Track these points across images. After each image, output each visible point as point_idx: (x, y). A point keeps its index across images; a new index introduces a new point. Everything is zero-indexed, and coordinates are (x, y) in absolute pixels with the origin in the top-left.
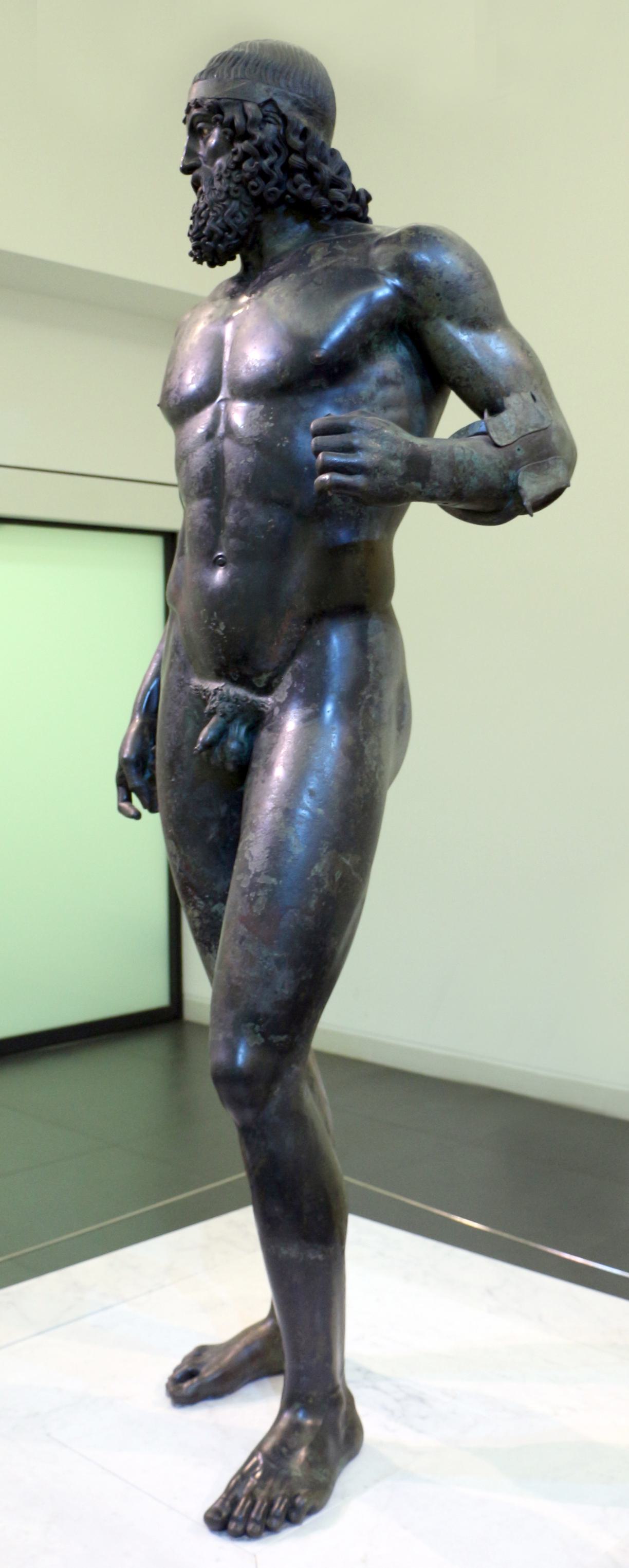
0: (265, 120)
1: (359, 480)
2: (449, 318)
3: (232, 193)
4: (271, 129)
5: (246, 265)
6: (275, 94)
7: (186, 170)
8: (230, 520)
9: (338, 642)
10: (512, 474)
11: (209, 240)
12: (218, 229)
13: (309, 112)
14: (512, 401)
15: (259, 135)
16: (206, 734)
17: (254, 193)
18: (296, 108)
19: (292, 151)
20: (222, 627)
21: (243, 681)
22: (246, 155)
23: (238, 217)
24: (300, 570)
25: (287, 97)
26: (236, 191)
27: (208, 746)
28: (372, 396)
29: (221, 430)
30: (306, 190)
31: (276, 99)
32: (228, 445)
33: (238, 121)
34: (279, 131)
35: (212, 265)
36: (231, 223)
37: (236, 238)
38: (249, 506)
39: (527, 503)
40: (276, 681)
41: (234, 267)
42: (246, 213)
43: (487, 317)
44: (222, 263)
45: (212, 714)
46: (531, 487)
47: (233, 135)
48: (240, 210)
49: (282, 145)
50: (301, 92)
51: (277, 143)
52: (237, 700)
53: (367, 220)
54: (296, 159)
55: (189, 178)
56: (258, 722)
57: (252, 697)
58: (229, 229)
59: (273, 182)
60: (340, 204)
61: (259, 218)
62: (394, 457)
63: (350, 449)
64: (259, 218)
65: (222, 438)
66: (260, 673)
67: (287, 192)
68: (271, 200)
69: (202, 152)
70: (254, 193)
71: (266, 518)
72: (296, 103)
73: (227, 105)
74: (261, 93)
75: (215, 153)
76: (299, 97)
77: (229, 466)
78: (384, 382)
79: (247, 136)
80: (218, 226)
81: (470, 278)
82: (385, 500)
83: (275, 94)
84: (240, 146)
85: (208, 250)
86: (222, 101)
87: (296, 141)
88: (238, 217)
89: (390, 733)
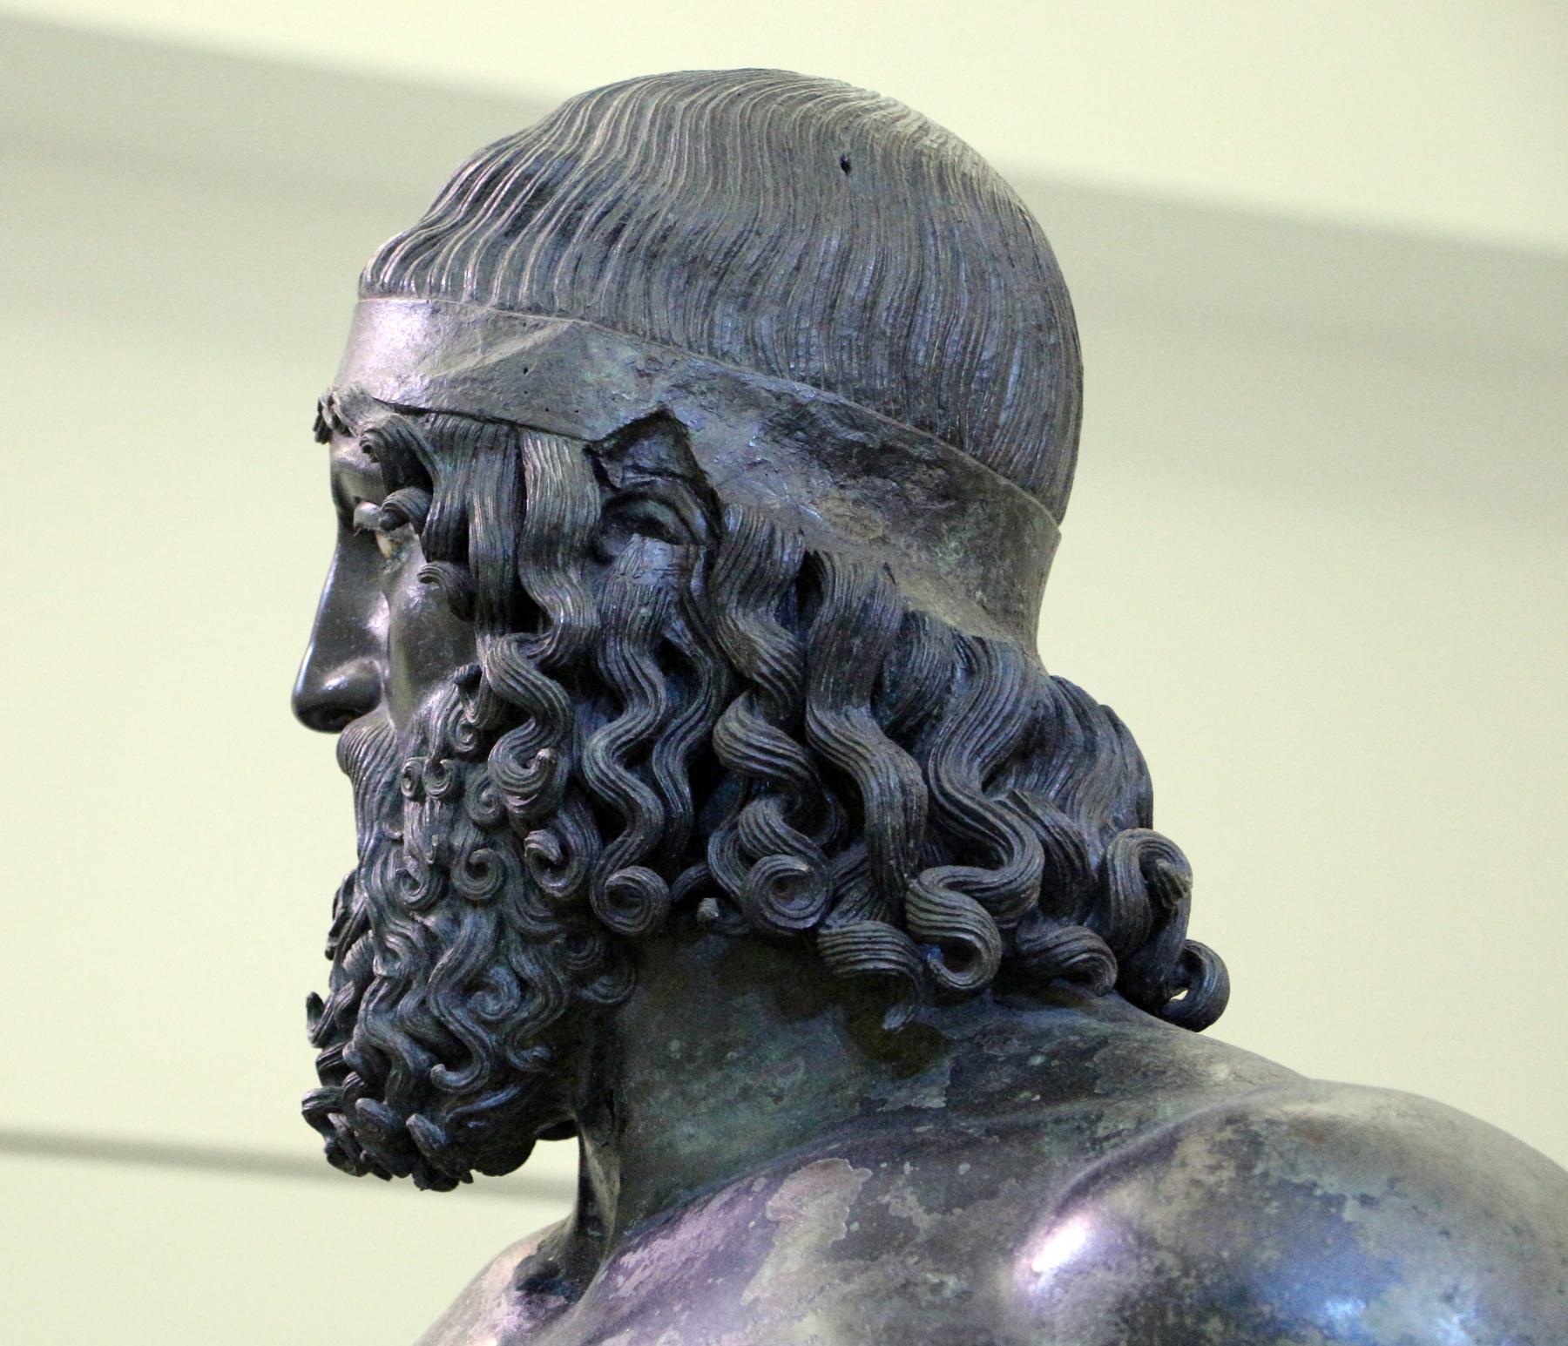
3: (460, 879)
6: (684, 387)
7: (321, 711)
11: (373, 1089)
12: (400, 1042)
17: (554, 886)
18: (790, 449)
22: (506, 713)
23: (494, 990)
25: (740, 395)
26: (478, 870)
30: (784, 883)
31: (683, 411)
34: (685, 571)
36: (459, 1019)
37: (497, 1086)
42: (530, 970)
48: (497, 954)
50: (821, 364)
51: (678, 631)
54: (744, 730)
58: (454, 1052)
59: (634, 839)
60: (960, 954)
61: (599, 990)
64: (599, 990)
67: (709, 887)
68: (625, 922)
70: (554, 886)
72: (792, 424)
73: (447, 443)
76: (806, 392)
80: (399, 1024)
83: (684, 387)
86: (420, 430)
87: (761, 636)
88: (494, 990)
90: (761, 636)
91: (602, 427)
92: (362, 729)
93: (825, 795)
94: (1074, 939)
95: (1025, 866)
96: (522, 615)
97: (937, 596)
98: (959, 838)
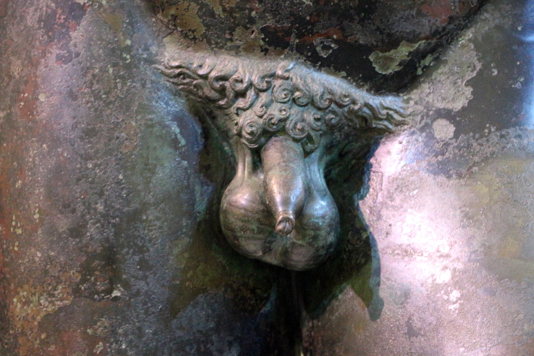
21: (350, 62)
40: (428, 60)
57: (362, 97)
66: (393, 43)
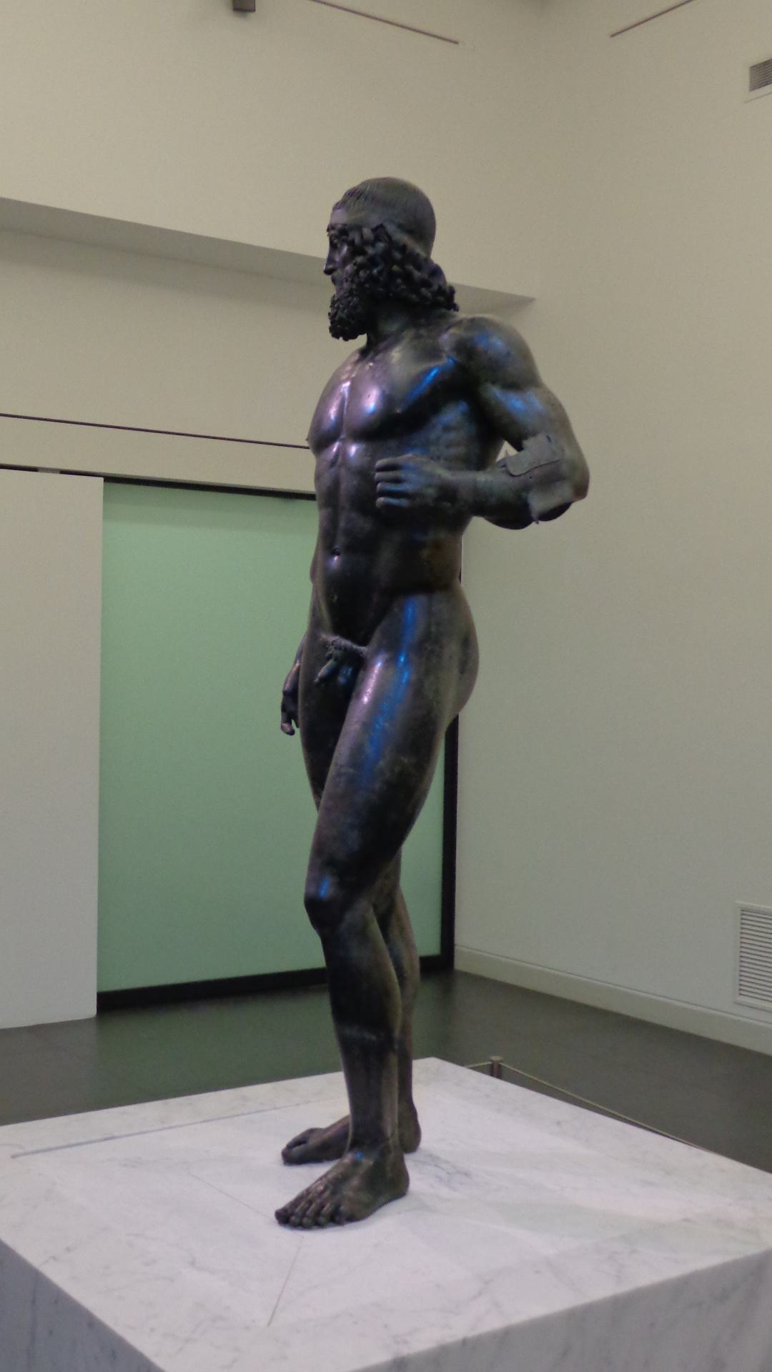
0: (377, 239)
1: (404, 502)
2: (493, 383)
4: (381, 245)
5: (369, 341)
7: (328, 272)
8: (342, 524)
9: (414, 610)
10: (524, 494)
13: (410, 232)
14: (528, 443)
15: (370, 251)
16: (323, 672)
19: (394, 262)
20: (336, 597)
24: (386, 558)
27: (324, 680)
28: (438, 438)
29: (340, 459)
32: (343, 471)
33: (357, 240)
35: (346, 339)
38: (354, 515)
39: (534, 515)
41: (362, 340)
43: (524, 380)
44: (354, 337)
45: (329, 658)
46: (538, 503)
47: (356, 250)
49: (386, 257)
52: (345, 649)
53: (455, 307)
54: (395, 268)
55: (329, 277)
56: (359, 665)
57: (355, 646)
62: (430, 486)
63: (397, 481)
65: (340, 466)
69: (337, 258)
71: (364, 525)
72: (400, 226)
74: (375, 220)
75: (345, 262)
77: (343, 486)
78: (447, 429)
79: (363, 253)
81: (508, 354)
82: (450, 512)
84: (359, 259)
85: (342, 329)
87: (398, 255)
89: (451, 675)
90: (398, 255)
91: (374, 226)
92: (335, 274)
93: (408, 277)
94: (441, 299)
95: (435, 288)
96: (363, 253)
97: (419, 250)
98: (427, 284)
